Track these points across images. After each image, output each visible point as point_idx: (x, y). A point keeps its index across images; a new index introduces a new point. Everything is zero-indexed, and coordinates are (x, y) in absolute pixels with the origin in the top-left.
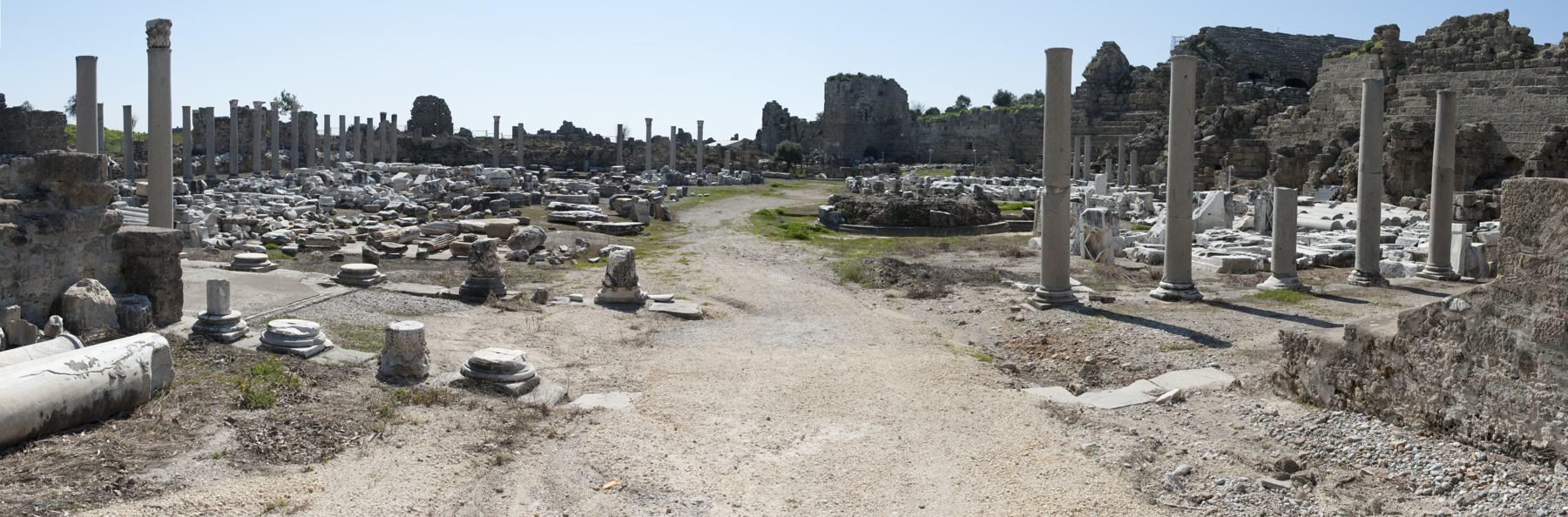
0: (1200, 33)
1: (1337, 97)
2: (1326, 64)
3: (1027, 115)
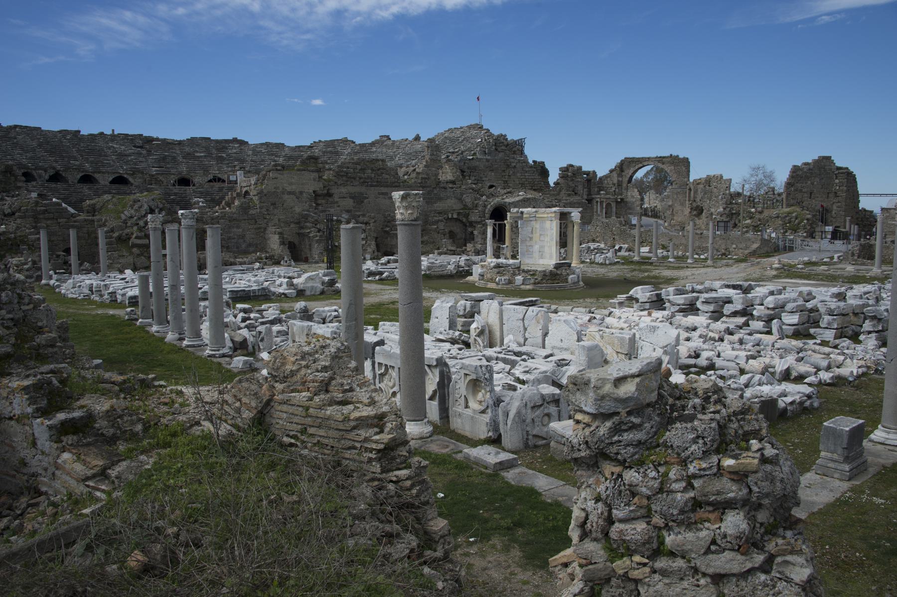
1: (286, 197)
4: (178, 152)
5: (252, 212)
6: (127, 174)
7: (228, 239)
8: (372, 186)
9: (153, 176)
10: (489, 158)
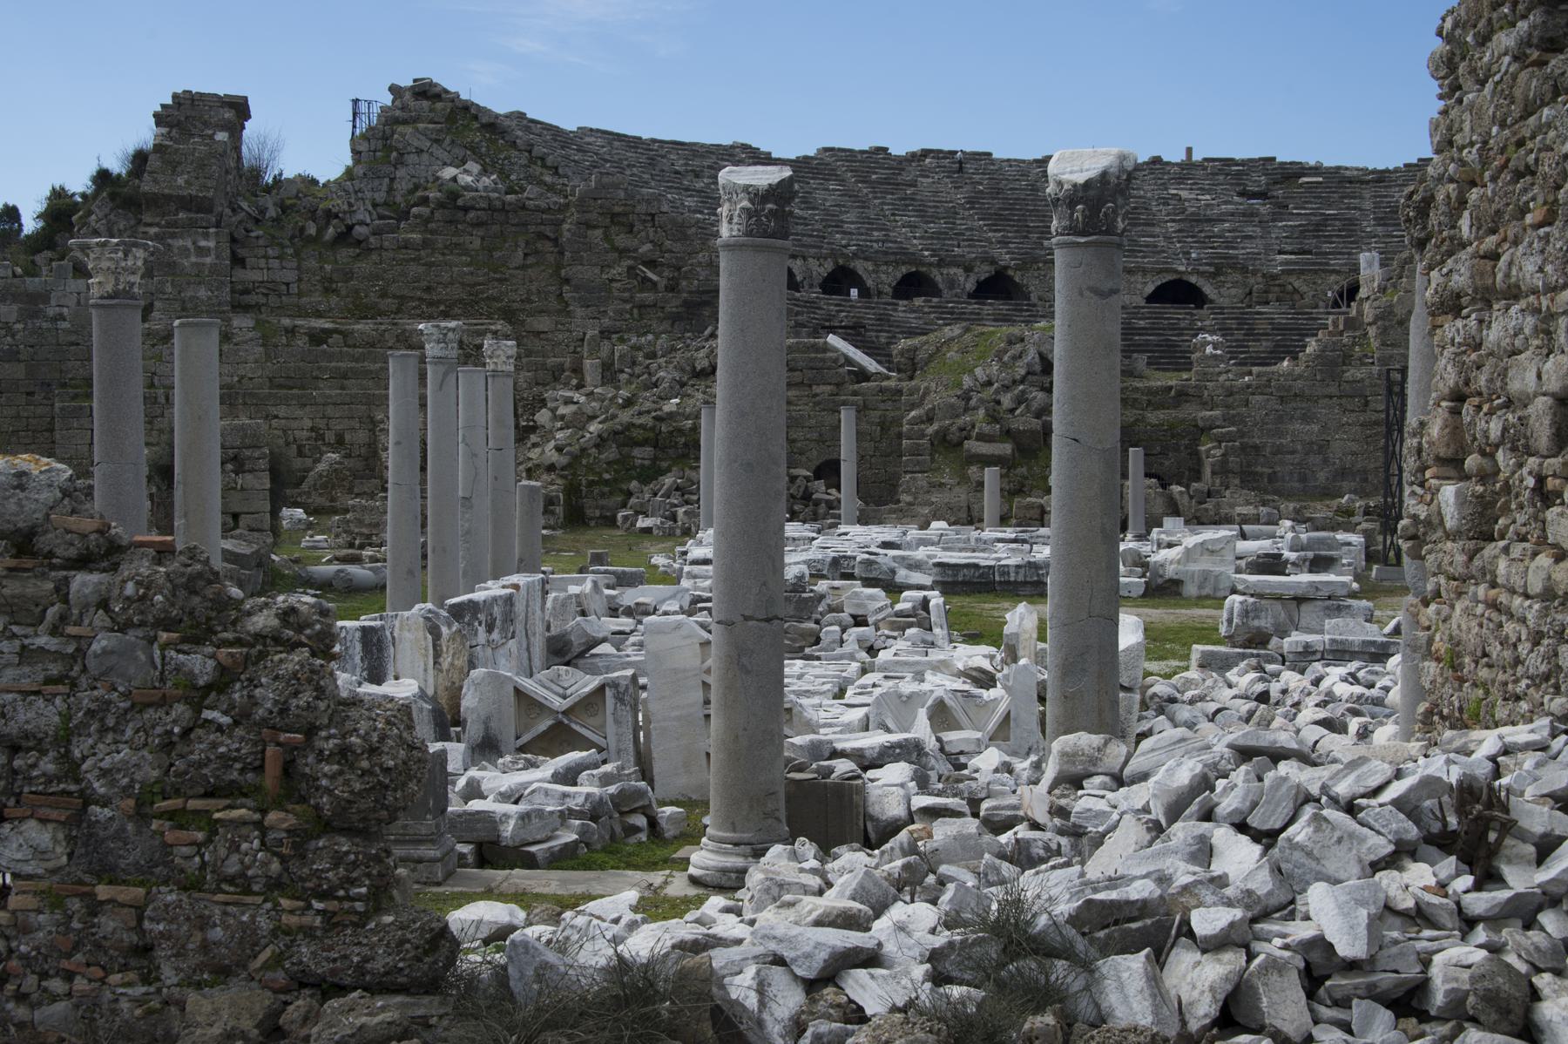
4: (1368, 205)
5: (1353, 373)
6: (1201, 274)
7: (1274, 454)
9: (1274, 277)
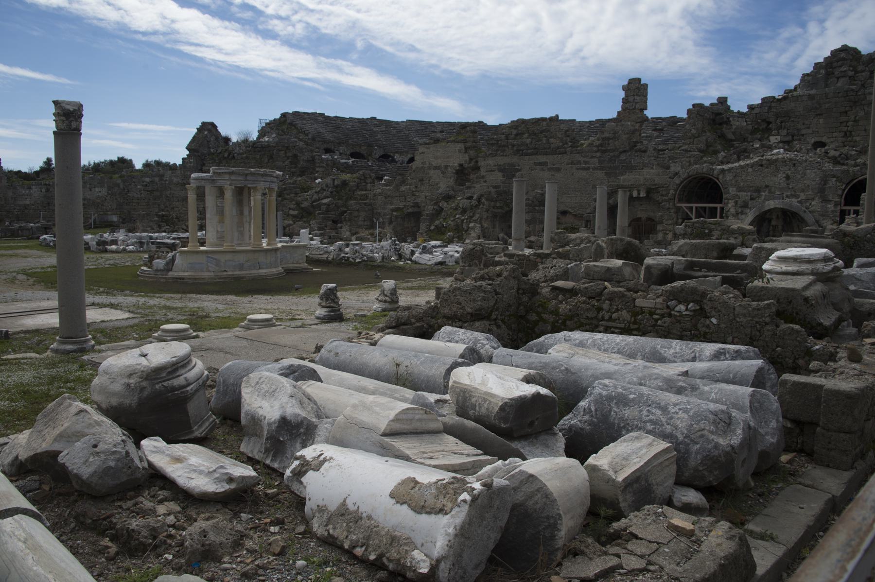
0: (281, 117)
1: (432, 172)
2: (422, 149)
3: (134, 180)
8: (527, 155)
10: (813, 92)
